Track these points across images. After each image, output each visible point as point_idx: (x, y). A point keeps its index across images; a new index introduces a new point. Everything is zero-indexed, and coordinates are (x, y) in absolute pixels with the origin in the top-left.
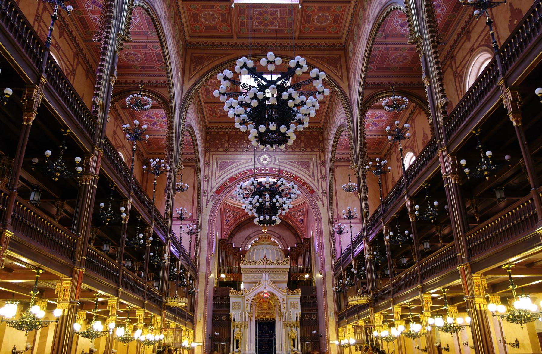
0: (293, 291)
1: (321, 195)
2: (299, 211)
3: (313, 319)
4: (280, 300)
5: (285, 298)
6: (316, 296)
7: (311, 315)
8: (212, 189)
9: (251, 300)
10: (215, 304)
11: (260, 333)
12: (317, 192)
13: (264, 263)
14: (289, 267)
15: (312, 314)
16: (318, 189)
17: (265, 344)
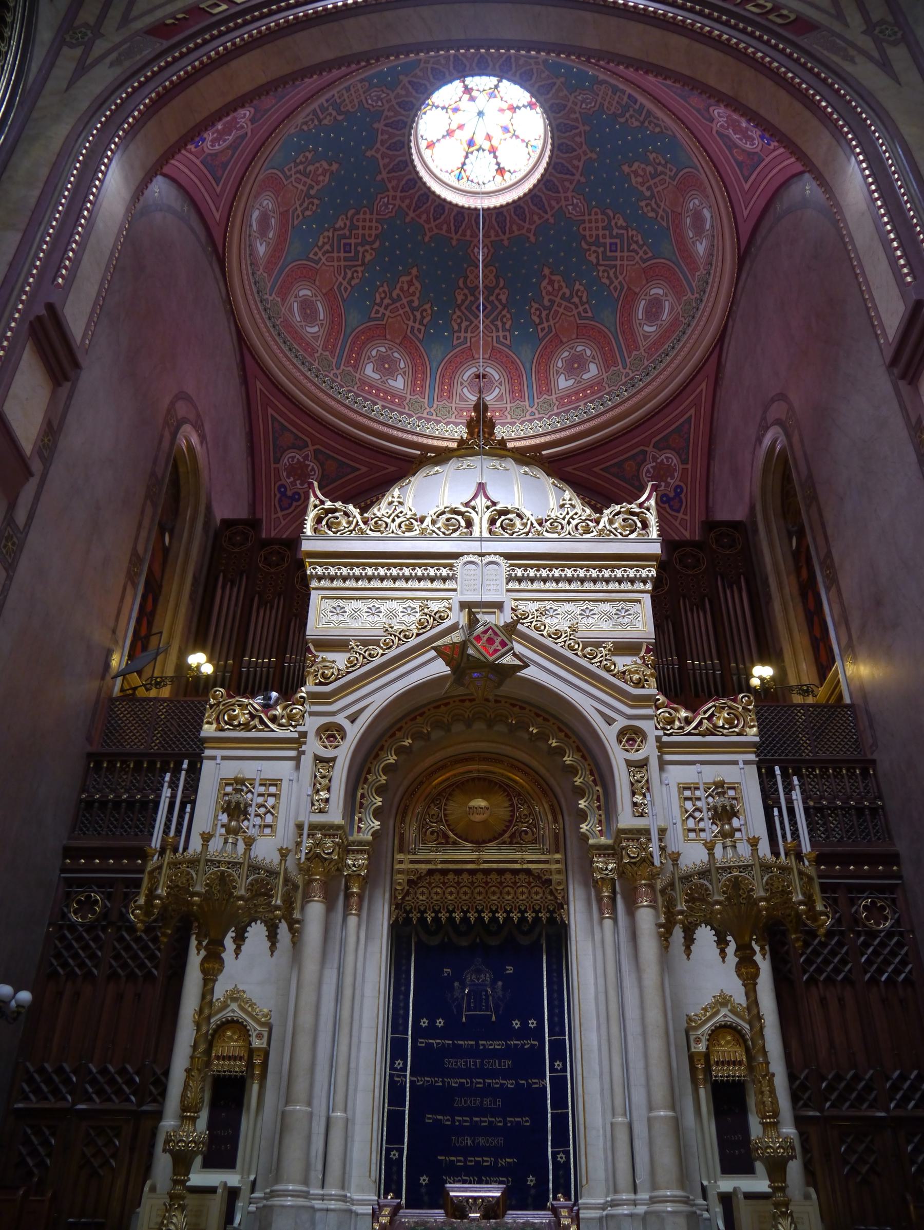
0: (693, 709)
1: (866, 42)
2: (662, 446)
3: (872, 934)
4: (608, 734)
5: (647, 726)
6: (867, 765)
7: (852, 902)
8: (125, 20)
9: (354, 732)
10: (89, 804)
11: (432, 1031)
12: (837, 27)
13: (469, 524)
14: (655, 549)
15: (862, 889)
16: (840, 16)
17: (476, 1130)
